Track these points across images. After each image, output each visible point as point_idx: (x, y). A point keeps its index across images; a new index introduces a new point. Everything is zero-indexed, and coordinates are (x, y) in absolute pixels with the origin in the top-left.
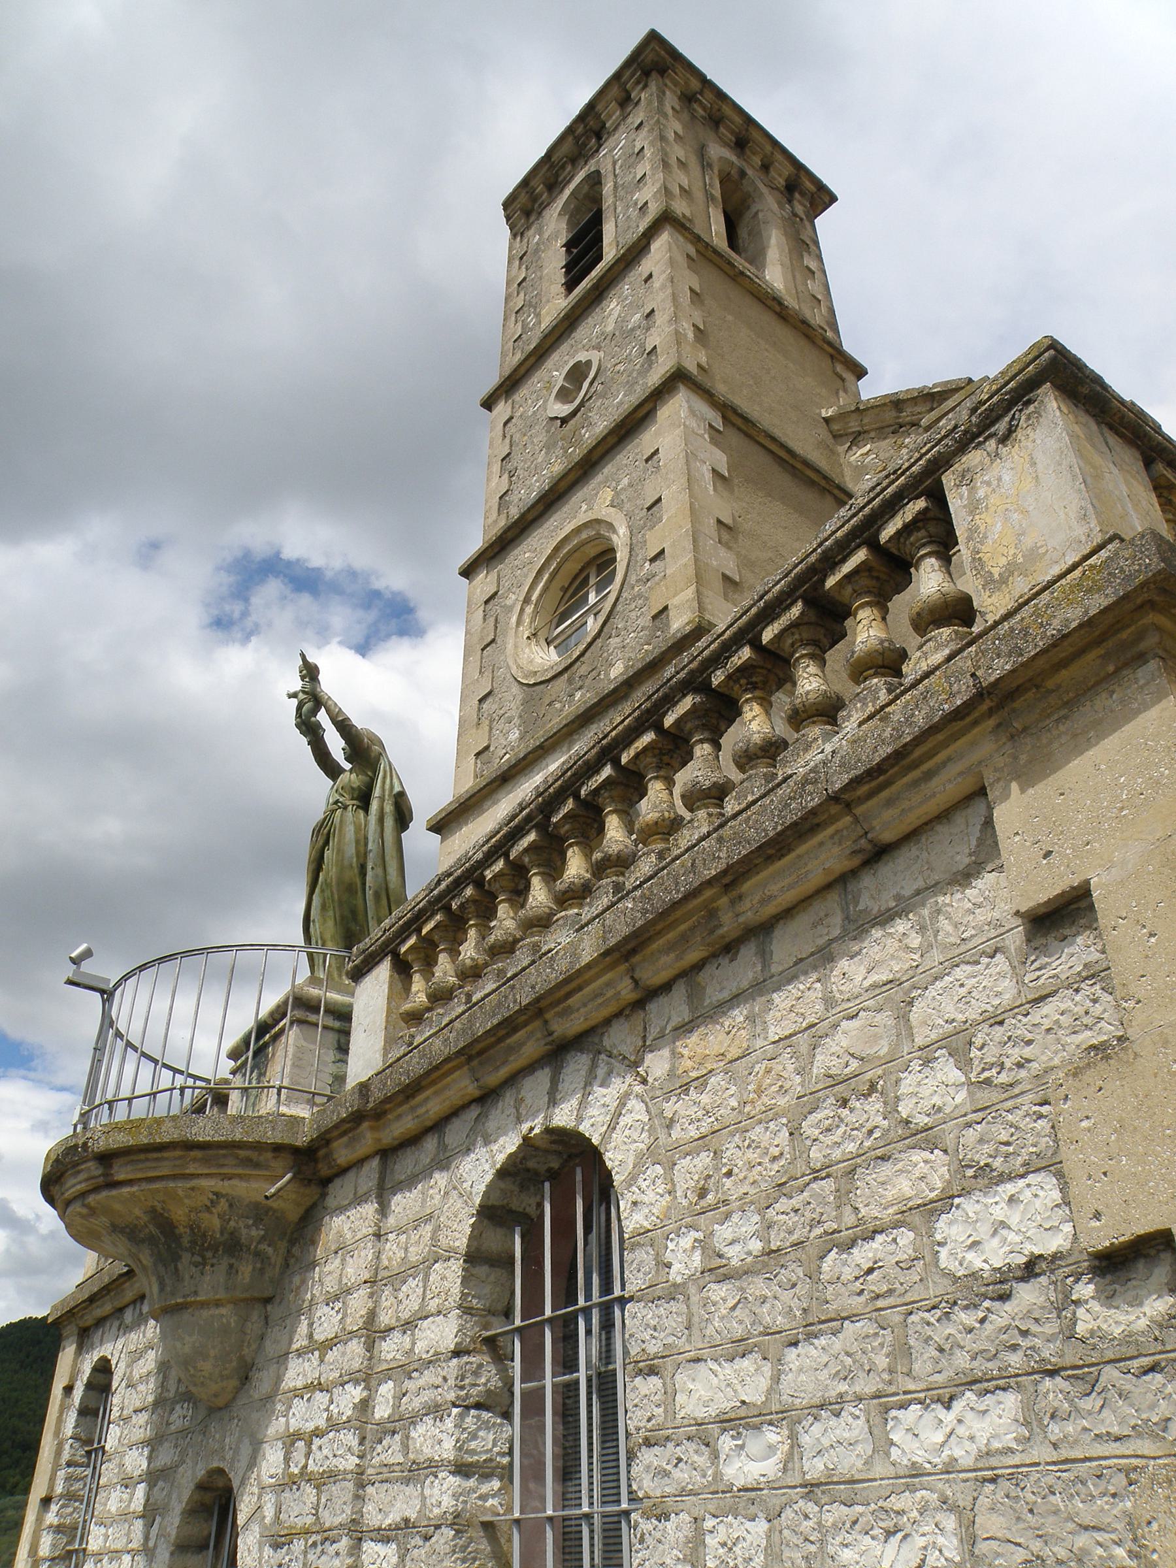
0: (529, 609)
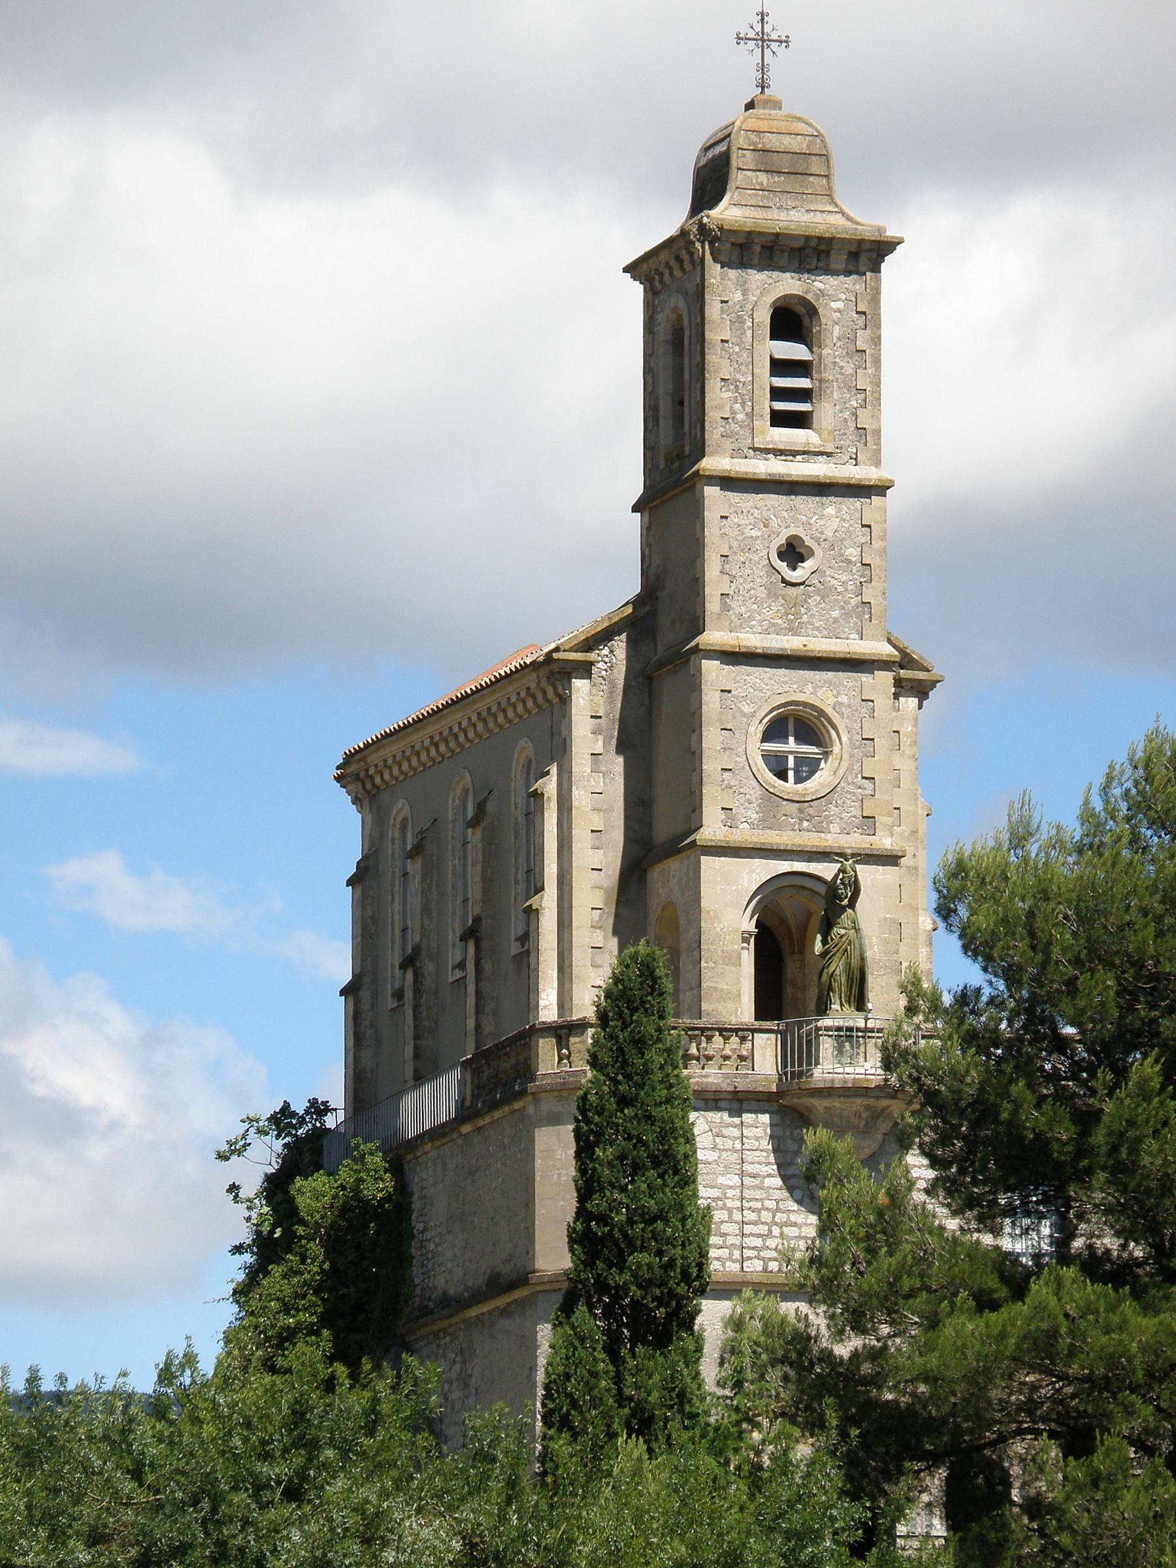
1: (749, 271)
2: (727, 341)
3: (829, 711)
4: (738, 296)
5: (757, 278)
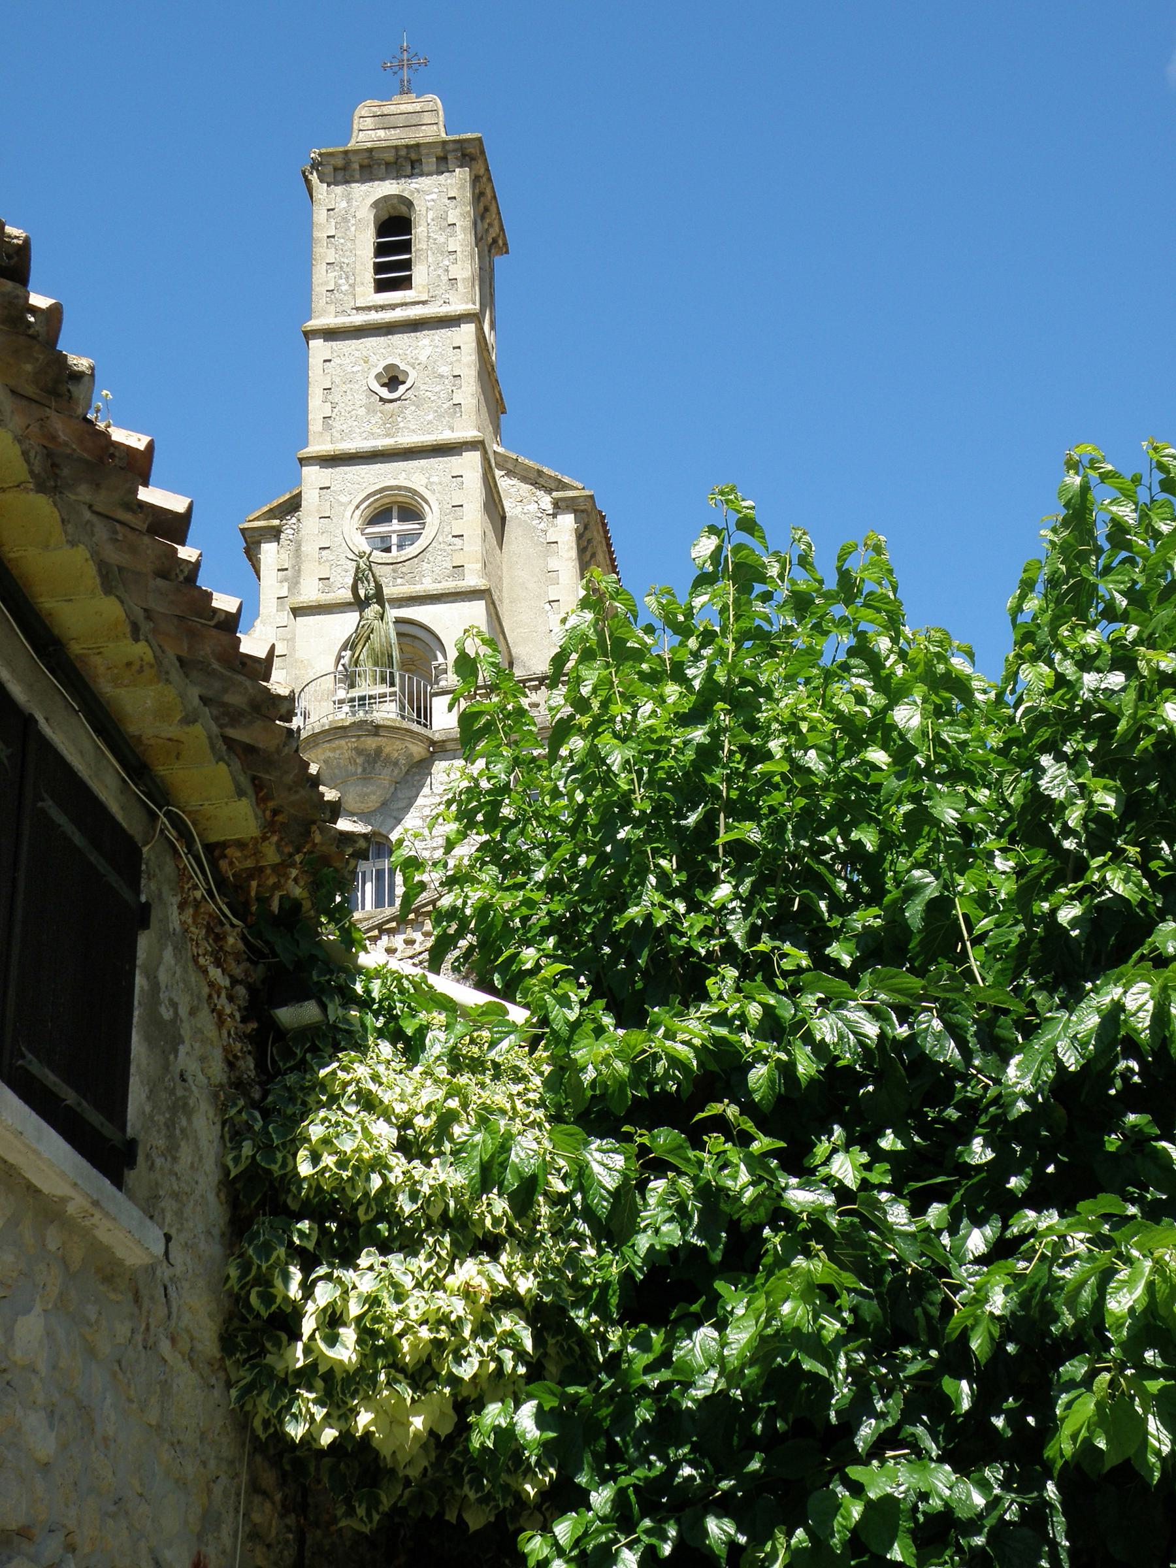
0: (358, 512)
1: (353, 185)
2: (333, 237)
3: (421, 490)
4: (344, 204)
5: (358, 189)
